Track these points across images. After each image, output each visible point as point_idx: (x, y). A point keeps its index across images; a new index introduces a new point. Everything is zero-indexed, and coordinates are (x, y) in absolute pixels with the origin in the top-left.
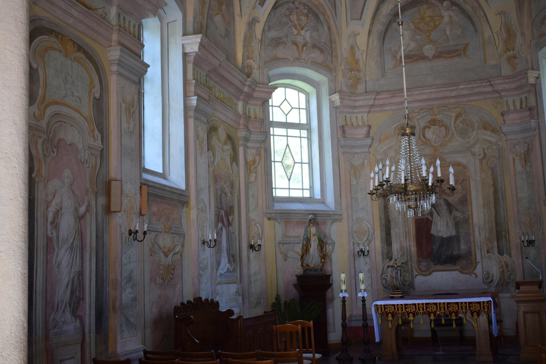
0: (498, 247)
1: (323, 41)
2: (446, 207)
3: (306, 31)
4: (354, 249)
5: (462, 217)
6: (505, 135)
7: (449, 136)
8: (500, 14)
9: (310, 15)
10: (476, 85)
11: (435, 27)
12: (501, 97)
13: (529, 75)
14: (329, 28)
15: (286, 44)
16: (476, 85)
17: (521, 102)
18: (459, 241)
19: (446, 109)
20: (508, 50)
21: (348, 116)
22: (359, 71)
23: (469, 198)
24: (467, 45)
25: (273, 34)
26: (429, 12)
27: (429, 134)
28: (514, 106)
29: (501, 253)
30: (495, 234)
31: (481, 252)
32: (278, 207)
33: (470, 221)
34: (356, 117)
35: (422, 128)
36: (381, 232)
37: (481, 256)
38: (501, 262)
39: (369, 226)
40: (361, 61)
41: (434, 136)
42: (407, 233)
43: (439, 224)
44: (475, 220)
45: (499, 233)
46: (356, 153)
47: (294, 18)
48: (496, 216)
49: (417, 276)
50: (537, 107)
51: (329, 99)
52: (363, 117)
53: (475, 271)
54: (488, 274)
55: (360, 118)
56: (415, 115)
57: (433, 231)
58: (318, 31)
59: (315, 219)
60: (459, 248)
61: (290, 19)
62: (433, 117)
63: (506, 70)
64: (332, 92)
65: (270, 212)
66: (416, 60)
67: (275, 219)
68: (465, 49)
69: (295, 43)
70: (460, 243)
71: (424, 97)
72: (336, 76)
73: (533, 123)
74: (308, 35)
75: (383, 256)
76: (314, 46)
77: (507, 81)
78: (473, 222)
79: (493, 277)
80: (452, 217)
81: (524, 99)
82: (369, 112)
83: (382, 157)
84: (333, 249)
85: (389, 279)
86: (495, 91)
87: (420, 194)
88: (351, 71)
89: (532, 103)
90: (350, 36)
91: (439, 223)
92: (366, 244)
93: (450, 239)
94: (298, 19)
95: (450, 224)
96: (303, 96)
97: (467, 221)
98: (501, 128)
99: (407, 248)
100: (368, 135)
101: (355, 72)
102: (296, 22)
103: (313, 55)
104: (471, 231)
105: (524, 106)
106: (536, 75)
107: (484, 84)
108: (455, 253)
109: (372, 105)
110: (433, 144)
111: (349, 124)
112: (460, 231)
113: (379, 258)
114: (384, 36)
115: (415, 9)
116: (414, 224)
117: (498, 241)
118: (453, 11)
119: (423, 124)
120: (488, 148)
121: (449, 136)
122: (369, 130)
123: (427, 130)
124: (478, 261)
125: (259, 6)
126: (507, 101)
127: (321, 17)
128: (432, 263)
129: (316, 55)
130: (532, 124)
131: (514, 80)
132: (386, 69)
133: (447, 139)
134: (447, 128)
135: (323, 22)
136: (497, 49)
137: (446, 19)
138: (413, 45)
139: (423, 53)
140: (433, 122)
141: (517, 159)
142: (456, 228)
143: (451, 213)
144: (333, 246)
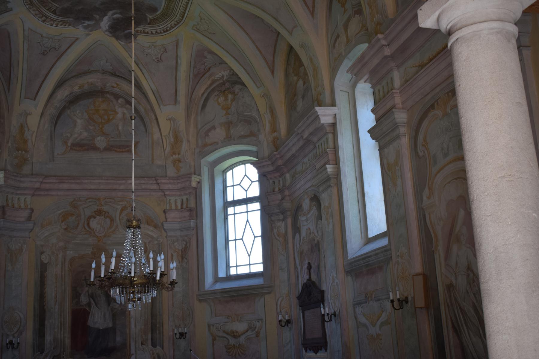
0: (152, 339)
4: (2, 341)
5: (120, 309)
6: (166, 232)
8: (170, 119)
10: (144, 182)
12: (165, 196)
13: (193, 178)
16: (144, 182)
17: (182, 202)
20: (174, 153)
21: (10, 196)
22: (26, 151)
27: (94, 224)
28: (176, 205)
29: (154, 345)
30: (150, 326)
31: (136, 344)
34: (18, 199)
37: (136, 348)
38: (153, 354)
41: (99, 226)
46: (14, 237)
50: (197, 209)
57: (90, 323)
62: (99, 208)
63: (171, 171)
71: (93, 187)
73: (192, 223)
77: (172, 181)
81: (185, 200)
82: (33, 195)
86: (160, 189)
87: (145, 287)
88: (18, 151)
89: (192, 205)
92: (16, 335)
93: (106, 331)
98: (162, 224)
100: (29, 219)
105: (184, 206)
106: (198, 180)
107: (151, 182)
109: (37, 189)
110: (97, 234)
111: (10, 205)
114: (56, 120)
117: (152, 334)
120: (149, 242)
122: (31, 213)
123: (92, 219)
124: (132, 353)
126: (170, 200)
130: (192, 223)
131: (179, 181)
134: (112, 220)
136: (164, 151)
137: (120, 115)
138: (85, 134)
140: (99, 213)
141: (175, 255)
143: (109, 304)
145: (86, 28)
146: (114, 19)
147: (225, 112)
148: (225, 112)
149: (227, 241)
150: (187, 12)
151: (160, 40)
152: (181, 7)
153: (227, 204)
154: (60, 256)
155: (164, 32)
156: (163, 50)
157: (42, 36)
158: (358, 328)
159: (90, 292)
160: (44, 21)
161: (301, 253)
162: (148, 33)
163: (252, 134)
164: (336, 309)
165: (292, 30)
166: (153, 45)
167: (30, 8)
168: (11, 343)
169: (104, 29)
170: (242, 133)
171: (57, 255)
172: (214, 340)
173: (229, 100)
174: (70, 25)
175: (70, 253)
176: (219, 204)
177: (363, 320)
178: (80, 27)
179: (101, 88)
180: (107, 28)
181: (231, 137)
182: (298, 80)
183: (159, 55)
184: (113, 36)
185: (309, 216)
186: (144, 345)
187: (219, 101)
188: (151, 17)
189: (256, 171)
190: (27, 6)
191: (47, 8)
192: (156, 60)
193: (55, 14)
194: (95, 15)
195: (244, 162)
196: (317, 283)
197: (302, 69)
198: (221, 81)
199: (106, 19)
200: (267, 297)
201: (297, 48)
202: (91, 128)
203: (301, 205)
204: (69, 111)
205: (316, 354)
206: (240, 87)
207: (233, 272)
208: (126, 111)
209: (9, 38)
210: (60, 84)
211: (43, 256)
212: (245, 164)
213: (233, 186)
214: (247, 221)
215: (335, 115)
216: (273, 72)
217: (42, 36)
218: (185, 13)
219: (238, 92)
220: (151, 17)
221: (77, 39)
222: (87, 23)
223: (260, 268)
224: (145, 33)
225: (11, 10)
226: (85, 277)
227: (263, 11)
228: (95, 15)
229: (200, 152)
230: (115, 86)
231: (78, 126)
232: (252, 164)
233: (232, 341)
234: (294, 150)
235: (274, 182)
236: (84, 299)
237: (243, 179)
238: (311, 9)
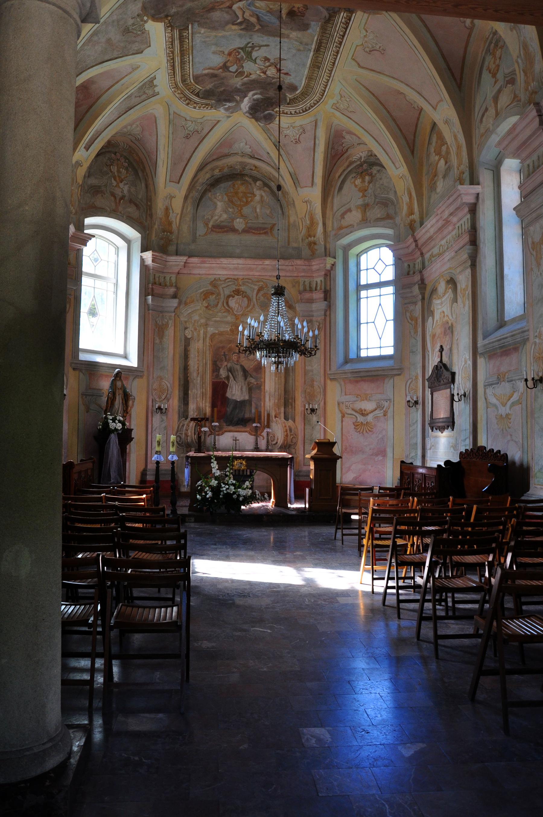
0: (285, 413)
1: (140, 197)
2: (242, 373)
3: (124, 185)
5: (255, 383)
7: (250, 307)
9: (130, 170)
11: (247, 203)
13: (327, 262)
14: (147, 186)
15: (105, 194)
17: (317, 284)
18: (251, 405)
19: (251, 281)
20: (310, 236)
21: (157, 275)
22: (171, 233)
24: (274, 225)
25: (93, 181)
26: (242, 188)
27: (232, 303)
28: (310, 287)
29: (286, 418)
30: (283, 401)
32: (83, 357)
34: (164, 278)
35: (226, 296)
36: (179, 391)
38: (285, 426)
39: (169, 385)
40: (174, 223)
41: (237, 305)
42: (203, 395)
43: (234, 388)
44: (267, 388)
45: (287, 400)
47: (114, 169)
48: (285, 385)
51: (141, 257)
52: (172, 278)
53: (263, 434)
54: (274, 436)
55: (168, 279)
56: (221, 283)
57: (228, 395)
58: (136, 187)
59: (121, 374)
60: (251, 411)
61: (110, 170)
62: (237, 287)
64: (144, 249)
65: (75, 362)
66: (227, 231)
67: (81, 370)
68: (272, 228)
69: (113, 195)
72: (148, 234)
74: (126, 189)
75: (179, 414)
76: (131, 201)
78: (264, 389)
79: (278, 439)
80: (246, 383)
81: (319, 282)
83: (186, 319)
84: (133, 405)
85: (183, 436)
88: (164, 232)
90: (166, 197)
93: (243, 403)
94: (119, 171)
95: (244, 389)
96: (112, 249)
97: (260, 387)
101: (167, 233)
102: (116, 173)
103: (129, 210)
104: (262, 397)
105: (318, 288)
106: (333, 263)
108: (247, 416)
110: (235, 313)
111: (157, 283)
113: (176, 417)
115: (230, 183)
117: (285, 408)
118: (264, 191)
119: (227, 292)
121: (250, 307)
123: (231, 298)
125: (84, 150)
127: (140, 175)
128: (225, 424)
129: (131, 210)
132: (197, 235)
133: (249, 309)
134: (249, 300)
135: (141, 179)
137: (258, 198)
138: (225, 216)
139: (234, 226)
140: (237, 292)
142: (249, 393)
143: (246, 379)
144: (133, 402)
145: (226, 110)
146: (254, 100)
147: (361, 194)
148: (361, 194)
149: (359, 324)
150: (327, 90)
151: (299, 121)
152: (322, 85)
153: (359, 287)
154: (202, 332)
155: (304, 112)
156: (301, 130)
157: (186, 120)
158: (487, 408)
159: (229, 366)
160: (188, 104)
161: (434, 336)
162: (287, 114)
163: (389, 217)
164: (466, 390)
165: (437, 106)
166: (291, 126)
167: (175, 92)
168: (160, 408)
169: (245, 111)
170: (379, 216)
171: (199, 331)
172: (343, 416)
173: (367, 182)
174: (212, 107)
175: (211, 330)
176: (352, 286)
177: (493, 400)
178: (222, 109)
179: (240, 171)
180: (247, 109)
181: (367, 220)
182: (439, 160)
183: (298, 136)
184: (253, 117)
185: (443, 300)
187: (356, 183)
188: (290, 96)
189: (392, 253)
190: (173, 90)
191: (191, 91)
192: (294, 142)
193: (198, 96)
194: (235, 97)
195: (379, 246)
196: (448, 366)
197: (444, 148)
198: (359, 163)
199: (246, 100)
200: (396, 378)
201: (441, 125)
202: (230, 210)
203: (436, 289)
204: (209, 194)
205: (442, 433)
206: (379, 168)
207: (363, 354)
208: (263, 194)
209: (156, 122)
210: (201, 168)
211: (187, 332)
212: (379, 248)
213: (367, 269)
214: (380, 305)
215: (478, 194)
216: (413, 152)
217: (186, 120)
218: (325, 91)
219: (375, 174)
220: (290, 96)
221: (218, 121)
222: (228, 104)
223: (390, 351)
224: (284, 113)
225: (158, 93)
226: (224, 352)
227: (407, 85)
228: (235, 97)
229: (335, 234)
230: (254, 168)
231: (219, 208)
232: (386, 246)
233: (360, 419)
234: (432, 231)
235: (409, 265)
236: (223, 373)
237: (377, 263)
238: (459, 81)
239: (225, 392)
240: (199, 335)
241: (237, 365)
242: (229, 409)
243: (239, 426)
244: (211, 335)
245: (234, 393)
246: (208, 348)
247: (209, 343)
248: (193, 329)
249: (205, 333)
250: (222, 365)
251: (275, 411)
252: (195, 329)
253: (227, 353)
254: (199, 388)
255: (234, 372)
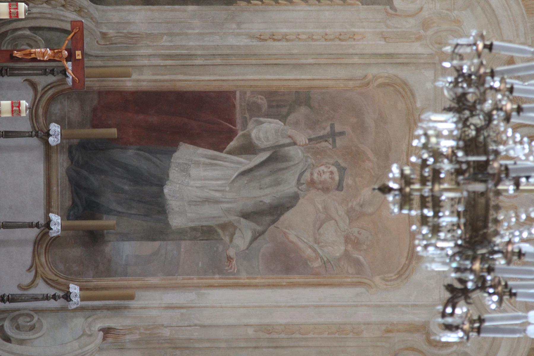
5: (231, 252)
23: (297, 279)
33: (217, 279)
42: (184, 59)
43: (209, 173)
49: (33, 85)
53: (41, 283)
57: (186, 152)
60: (126, 237)
70: (142, 239)
78: (211, 286)
79: (21, 342)
80: (232, 218)
91: (216, 173)
95: (208, 211)
97: (219, 269)
99: (132, 57)
104: (180, 280)
112: (183, 243)
116: (213, 87)
142: (193, 229)
143: (246, 216)
154: (417, 48)
159: (292, 151)
171: (419, 39)
186: (104, 339)
226: (342, 134)
236: (265, 131)
239: (194, 139)
240: (403, 37)
241: (299, 182)
242: (130, 156)
243: (68, 194)
244: (405, 83)
245: (194, 172)
246: (358, 73)
247: (376, 78)
248: (425, 14)
249: (410, 61)
250: (296, 124)
251: (131, 330)
252: (426, 25)
253: (339, 142)
254: (208, 41)
255: (273, 172)
